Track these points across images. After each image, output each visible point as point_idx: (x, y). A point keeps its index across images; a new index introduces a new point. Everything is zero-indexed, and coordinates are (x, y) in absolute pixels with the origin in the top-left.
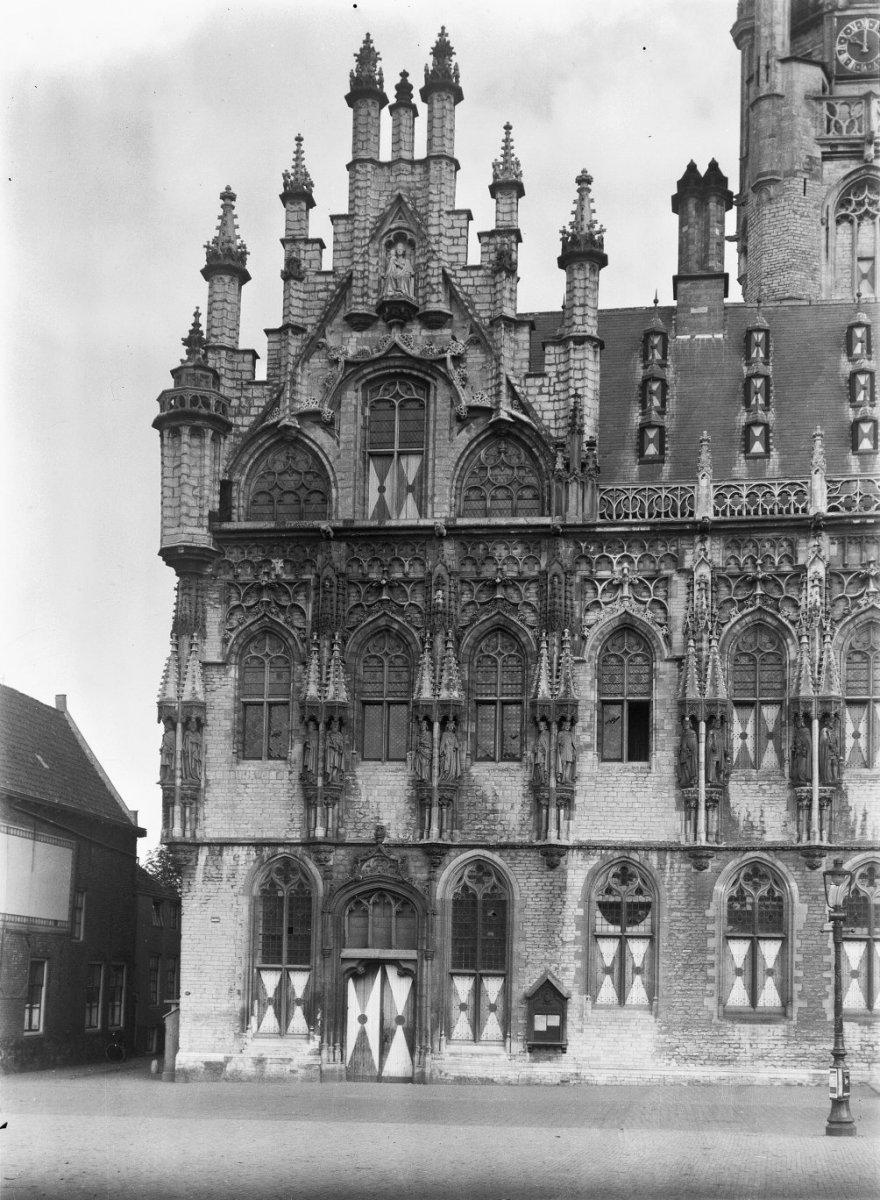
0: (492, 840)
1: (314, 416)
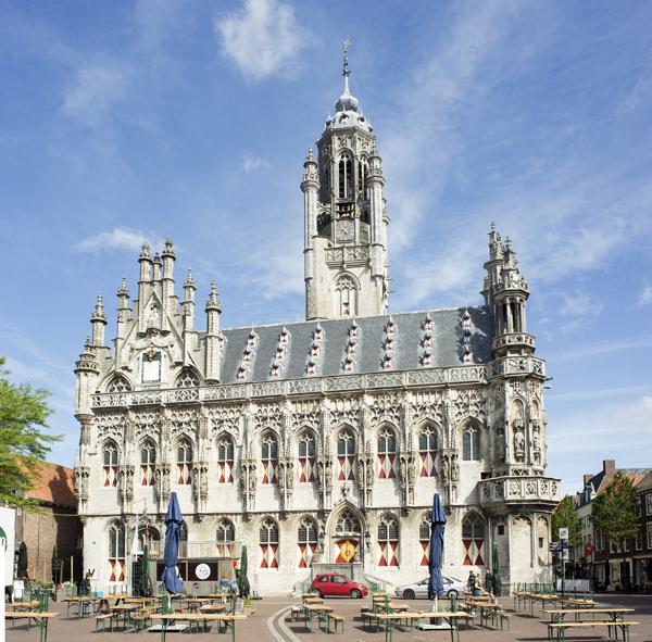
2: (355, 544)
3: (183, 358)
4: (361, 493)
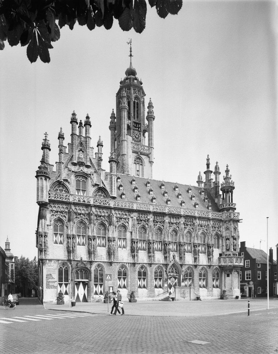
2: (175, 278)
4: (181, 258)
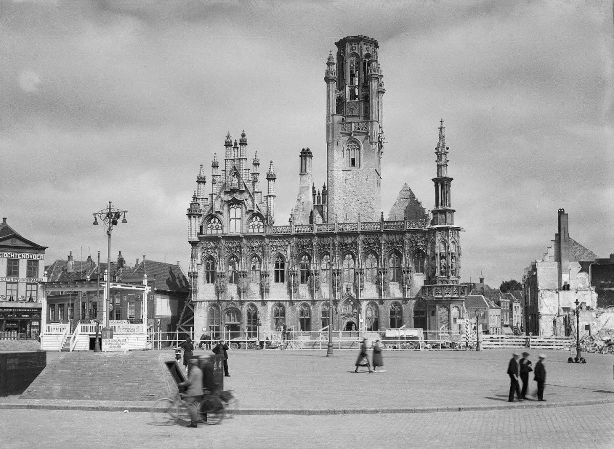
0: (253, 300)
1: (219, 212)
3: (254, 207)
